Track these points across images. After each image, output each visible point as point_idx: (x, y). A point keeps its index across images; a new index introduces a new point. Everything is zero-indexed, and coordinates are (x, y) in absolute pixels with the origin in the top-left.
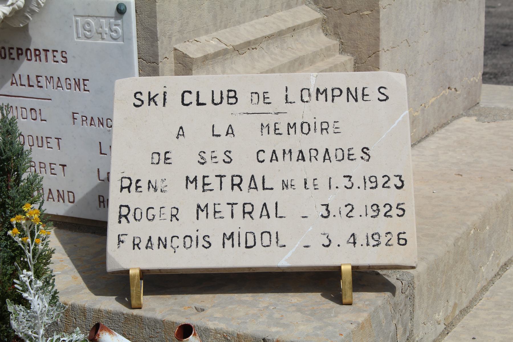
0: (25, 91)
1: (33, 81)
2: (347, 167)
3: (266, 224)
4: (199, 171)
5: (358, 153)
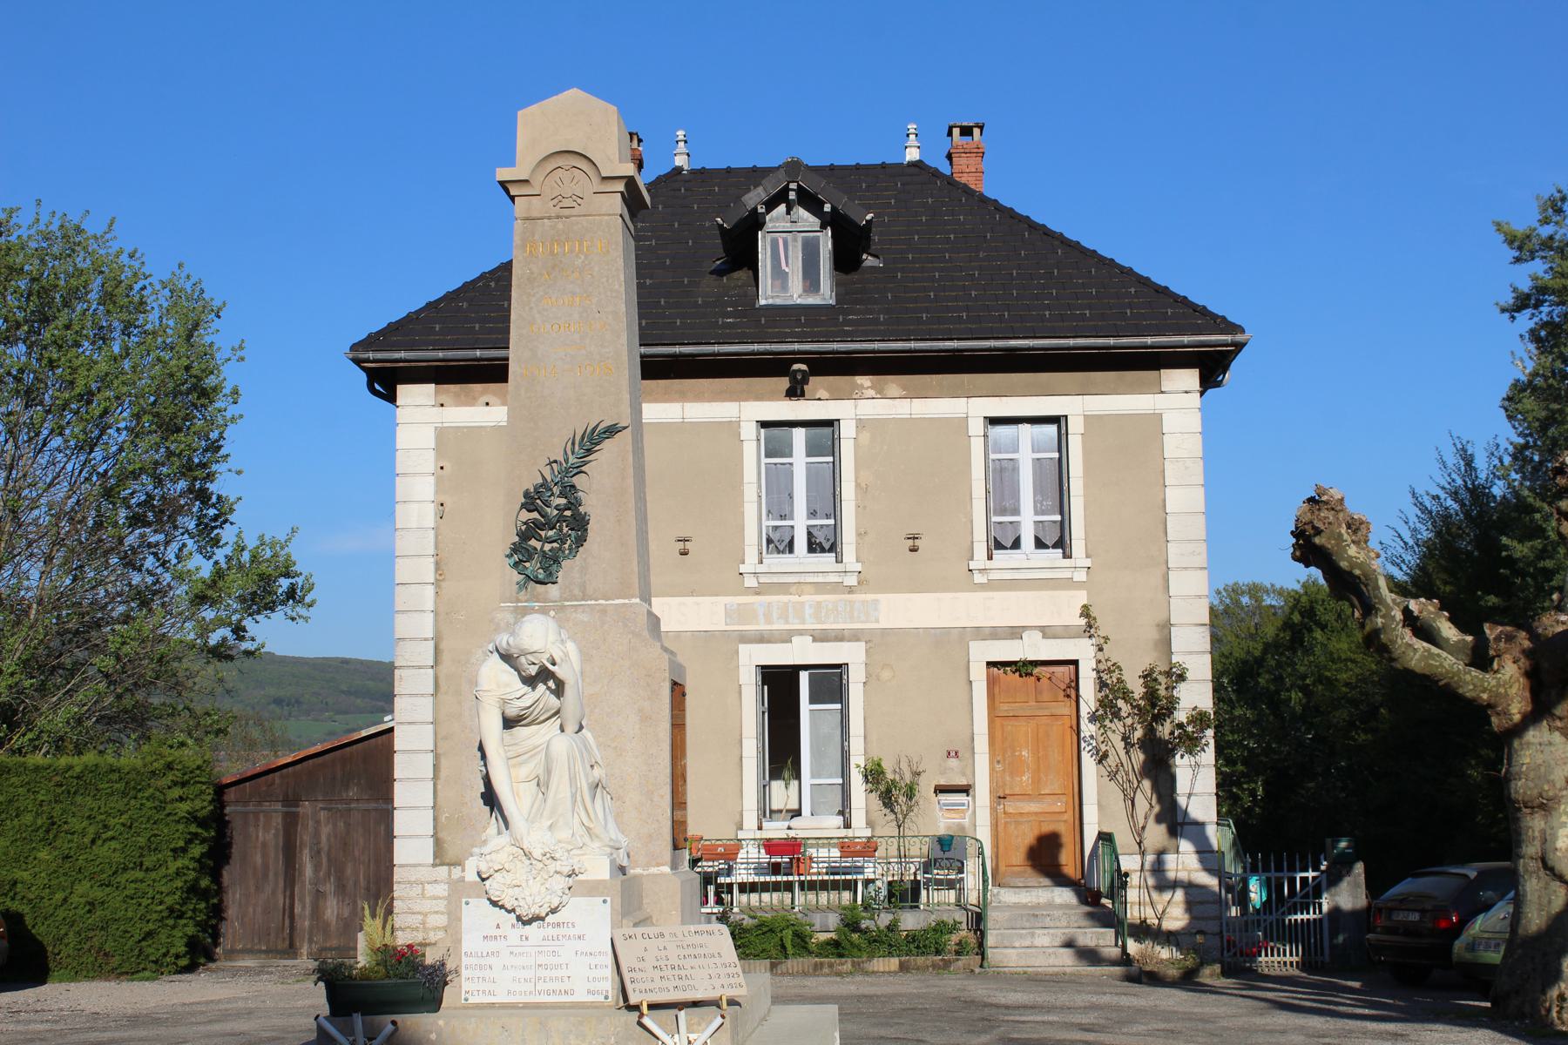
0: (554, 943)
1: (555, 938)
2: (713, 960)
3: (688, 982)
4: (658, 964)
5: (716, 955)
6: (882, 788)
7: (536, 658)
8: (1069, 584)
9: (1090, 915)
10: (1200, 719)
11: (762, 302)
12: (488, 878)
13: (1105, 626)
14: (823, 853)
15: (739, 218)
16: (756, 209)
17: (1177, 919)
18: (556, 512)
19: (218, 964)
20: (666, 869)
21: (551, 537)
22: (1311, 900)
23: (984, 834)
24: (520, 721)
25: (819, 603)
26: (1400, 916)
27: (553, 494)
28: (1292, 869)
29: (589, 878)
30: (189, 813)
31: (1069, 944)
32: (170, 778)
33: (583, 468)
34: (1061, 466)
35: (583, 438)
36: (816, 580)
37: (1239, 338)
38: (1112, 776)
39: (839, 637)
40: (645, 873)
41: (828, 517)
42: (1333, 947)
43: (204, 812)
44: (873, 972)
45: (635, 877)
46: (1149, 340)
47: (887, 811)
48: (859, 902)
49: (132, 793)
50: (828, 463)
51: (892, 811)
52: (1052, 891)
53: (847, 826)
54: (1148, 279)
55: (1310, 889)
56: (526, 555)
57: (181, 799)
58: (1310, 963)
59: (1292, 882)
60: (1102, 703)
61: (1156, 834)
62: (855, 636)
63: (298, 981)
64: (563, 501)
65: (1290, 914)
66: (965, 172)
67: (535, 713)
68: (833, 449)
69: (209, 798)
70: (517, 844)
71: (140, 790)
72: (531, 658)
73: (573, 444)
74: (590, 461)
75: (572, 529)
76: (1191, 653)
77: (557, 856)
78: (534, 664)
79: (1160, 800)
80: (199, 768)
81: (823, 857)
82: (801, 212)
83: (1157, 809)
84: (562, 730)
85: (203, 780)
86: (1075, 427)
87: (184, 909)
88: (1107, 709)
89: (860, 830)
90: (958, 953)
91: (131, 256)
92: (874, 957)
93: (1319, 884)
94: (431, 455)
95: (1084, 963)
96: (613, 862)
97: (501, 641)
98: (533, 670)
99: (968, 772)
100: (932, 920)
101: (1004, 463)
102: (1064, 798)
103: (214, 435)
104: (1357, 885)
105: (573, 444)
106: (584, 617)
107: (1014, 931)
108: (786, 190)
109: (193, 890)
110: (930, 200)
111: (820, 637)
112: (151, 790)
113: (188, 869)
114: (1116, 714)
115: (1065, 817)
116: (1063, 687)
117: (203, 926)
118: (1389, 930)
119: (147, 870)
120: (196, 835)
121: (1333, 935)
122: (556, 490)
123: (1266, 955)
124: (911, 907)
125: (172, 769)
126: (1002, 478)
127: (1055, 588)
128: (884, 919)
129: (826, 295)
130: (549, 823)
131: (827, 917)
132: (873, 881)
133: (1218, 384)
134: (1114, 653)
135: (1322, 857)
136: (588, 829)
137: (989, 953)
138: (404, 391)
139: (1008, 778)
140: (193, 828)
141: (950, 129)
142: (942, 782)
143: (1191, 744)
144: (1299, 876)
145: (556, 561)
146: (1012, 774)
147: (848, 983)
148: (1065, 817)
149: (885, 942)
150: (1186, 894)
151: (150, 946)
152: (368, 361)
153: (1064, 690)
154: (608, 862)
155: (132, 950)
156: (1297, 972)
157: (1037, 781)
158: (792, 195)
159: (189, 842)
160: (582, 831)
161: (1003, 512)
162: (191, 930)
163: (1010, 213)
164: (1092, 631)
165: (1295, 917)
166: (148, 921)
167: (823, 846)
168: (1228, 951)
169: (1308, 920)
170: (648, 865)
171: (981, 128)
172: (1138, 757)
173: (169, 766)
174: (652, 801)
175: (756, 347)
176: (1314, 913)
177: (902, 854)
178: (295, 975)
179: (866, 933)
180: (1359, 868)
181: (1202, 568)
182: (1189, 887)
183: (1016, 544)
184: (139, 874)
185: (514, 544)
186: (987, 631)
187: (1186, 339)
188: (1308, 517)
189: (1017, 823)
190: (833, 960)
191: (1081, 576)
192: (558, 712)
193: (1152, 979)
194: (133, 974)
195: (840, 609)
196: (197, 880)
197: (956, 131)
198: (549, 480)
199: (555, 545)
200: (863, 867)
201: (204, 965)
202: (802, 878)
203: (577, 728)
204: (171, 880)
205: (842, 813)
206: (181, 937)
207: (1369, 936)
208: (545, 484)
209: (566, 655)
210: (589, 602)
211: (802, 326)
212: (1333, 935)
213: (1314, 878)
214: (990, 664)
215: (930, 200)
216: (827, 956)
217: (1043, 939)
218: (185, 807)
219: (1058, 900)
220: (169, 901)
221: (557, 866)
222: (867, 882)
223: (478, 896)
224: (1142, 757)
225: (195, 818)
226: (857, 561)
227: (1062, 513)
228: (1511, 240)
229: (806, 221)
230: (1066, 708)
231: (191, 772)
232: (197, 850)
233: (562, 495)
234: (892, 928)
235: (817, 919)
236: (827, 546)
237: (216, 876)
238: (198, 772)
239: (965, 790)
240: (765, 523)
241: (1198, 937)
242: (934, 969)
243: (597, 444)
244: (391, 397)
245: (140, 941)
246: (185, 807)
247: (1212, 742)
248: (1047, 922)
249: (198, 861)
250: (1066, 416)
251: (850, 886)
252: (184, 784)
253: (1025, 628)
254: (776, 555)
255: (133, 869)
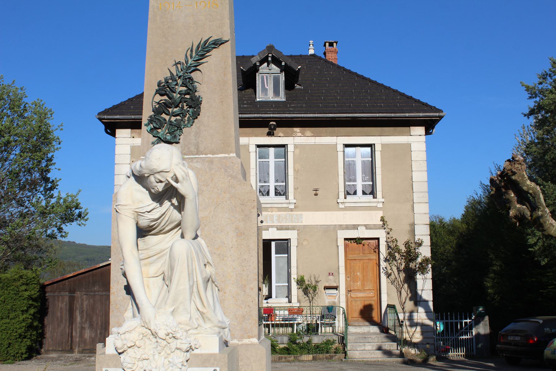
6: (304, 287)
7: (163, 177)
8: (376, 208)
9: (387, 337)
10: (426, 261)
11: (258, 100)
12: (123, 352)
13: (390, 224)
14: (282, 312)
15: (249, 67)
16: (256, 64)
17: (417, 338)
18: (179, 95)
19: (42, 356)
20: (255, 340)
21: (175, 112)
22: (469, 331)
23: (343, 304)
24: (150, 231)
25: (280, 215)
26: (511, 338)
27: (177, 84)
28: (461, 319)
29: (203, 352)
30: (29, 296)
31: (380, 349)
32: (21, 282)
33: (198, 67)
34: (373, 163)
35: (198, 47)
36: (278, 206)
37: (441, 114)
38: (393, 282)
39: (287, 228)
40: (240, 343)
41: (283, 182)
42: (477, 348)
43: (35, 296)
44: (302, 361)
45: (235, 347)
46: (407, 115)
47: (306, 296)
48: (295, 332)
49: (6, 288)
50: (283, 161)
51: (308, 296)
52: (370, 327)
53: (290, 302)
54: (404, 94)
55: (468, 326)
56: (159, 124)
57: (26, 290)
58: (468, 355)
59: (461, 323)
60: (390, 254)
61: (409, 305)
62: (293, 228)
63: (71, 364)
64: (185, 88)
65: (461, 336)
66: (330, 57)
67: (162, 224)
68: (285, 156)
69: (37, 290)
70: (145, 325)
71: (9, 287)
72: (158, 176)
73: (192, 51)
74: (203, 63)
75: (190, 107)
76: (422, 235)
77: (178, 335)
78: (161, 182)
79: (411, 292)
80: (34, 278)
81: (281, 314)
82: (273, 66)
83: (410, 295)
84: (182, 236)
85: (35, 282)
86: (378, 148)
87: (26, 335)
88: (391, 258)
89: (295, 304)
90: (335, 353)
91: (21, 89)
92: (302, 354)
93: (471, 325)
94: (129, 157)
95: (385, 356)
96: (221, 338)
97: (135, 166)
98: (160, 187)
99: (337, 281)
100: (325, 339)
101: (351, 162)
102: (373, 291)
103: (50, 155)
104: (486, 325)
105: (192, 51)
106: (198, 165)
107: (357, 344)
108: (268, 57)
109: (30, 327)
110: (319, 67)
111: (280, 228)
112: (13, 287)
113: (28, 318)
114: (394, 258)
115: (374, 299)
116: (373, 248)
117: (35, 341)
118: (505, 343)
119: (11, 319)
120: (32, 305)
121: (477, 344)
122: (180, 82)
123: (452, 352)
124: (315, 334)
125: (22, 278)
126: (349, 169)
127: (370, 210)
128: (306, 339)
129: (282, 98)
130: (172, 309)
131: (283, 338)
132: (300, 324)
133: (431, 134)
134: (393, 235)
135: (473, 314)
136: (202, 314)
137: (348, 352)
138: (120, 133)
139: (352, 284)
140: (31, 302)
141: (325, 43)
142: (327, 285)
143: (422, 269)
144: (464, 321)
145: (179, 128)
146: (354, 282)
147: (294, 365)
148: (374, 299)
149: (307, 348)
150: (421, 328)
151: (11, 350)
152: (104, 119)
153: (374, 250)
154: (218, 339)
155: (4, 351)
156: (463, 359)
157: (363, 285)
158: (270, 59)
159: (29, 308)
160: (197, 315)
161: (350, 181)
162: (29, 343)
163: (349, 72)
164: (385, 226)
165: (463, 337)
166: (11, 340)
167: (282, 310)
168: (437, 350)
169: (467, 338)
170: (242, 338)
171: (337, 43)
172: (403, 275)
173: (21, 277)
174: (245, 292)
175: (256, 115)
176: (470, 336)
177: (312, 313)
178: (70, 361)
179: (299, 344)
180: (487, 318)
181: (426, 203)
182: (423, 325)
183: (355, 193)
184: (8, 321)
185: (151, 117)
186: (344, 226)
187: (421, 114)
188: (510, 167)
189: (356, 301)
190: (286, 356)
191: (380, 205)
192: (179, 225)
193: (411, 362)
194: (4, 361)
195: (287, 218)
196: (32, 323)
197: (327, 44)
198: (175, 74)
199: (178, 118)
200: (296, 318)
201: (35, 356)
202: (273, 322)
203: (194, 236)
204: (21, 323)
205: (288, 297)
206: (24, 346)
207: (498, 346)
208: (172, 77)
209: (187, 175)
210: (201, 156)
211: (274, 108)
212: (477, 344)
213: (469, 322)
214: (345, 239)
215: (319, 67)
216: (283, 354)
217: (369, 347)
218: (27, 293)
219: (372, 331)
220: (19, 331)
221: (178, 343)
222: (298, 324)
223: (116, 366)
224: (404, 275)
225: (32, 298)
226: (294, 199)
227: (372, 181)
228: (528, 89)
229: (275, 69)
230: (374, 257)
231: (30, 279)
232: (32, 311)
233: (184, 85)
234: (309, 342)
235: (279, 339)
236: (282, 193)
237: (41, 321)
238: (33, 279)
239: (336, 288)
240: (259, 184)
241: (427, 345)
242: (326, 359)
243: (208, 51)
244: (113, 134)
245: (7, 348)
246: (27, 293)
247: (431, 269)
248: (370, 340)
249: (33, 315)
250: (374, 144)
251: (292, 326)
252: (27, 284)
253: (359, 225)
254: (262, 197)
255: (5, 318)
